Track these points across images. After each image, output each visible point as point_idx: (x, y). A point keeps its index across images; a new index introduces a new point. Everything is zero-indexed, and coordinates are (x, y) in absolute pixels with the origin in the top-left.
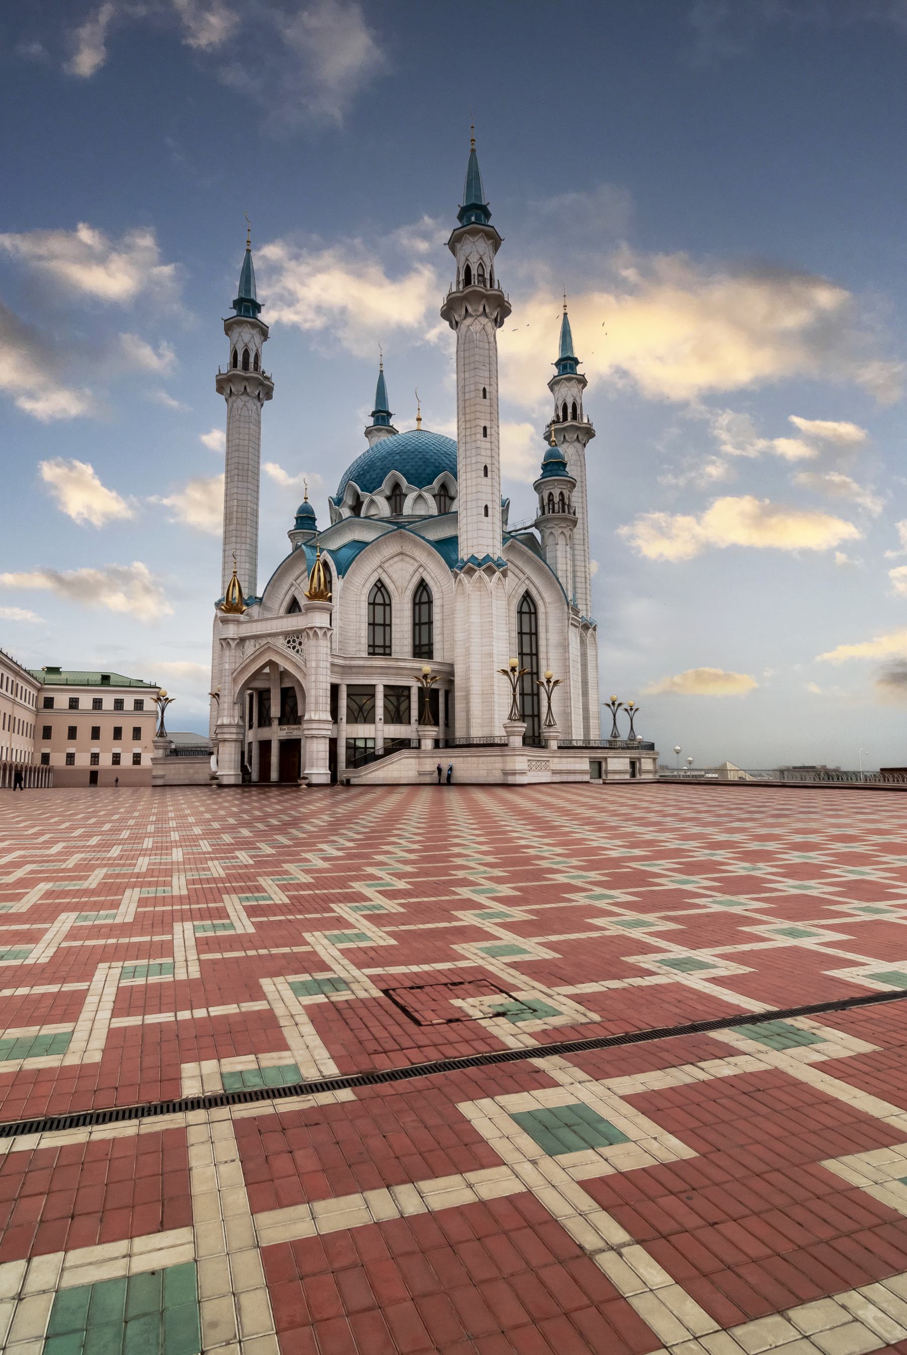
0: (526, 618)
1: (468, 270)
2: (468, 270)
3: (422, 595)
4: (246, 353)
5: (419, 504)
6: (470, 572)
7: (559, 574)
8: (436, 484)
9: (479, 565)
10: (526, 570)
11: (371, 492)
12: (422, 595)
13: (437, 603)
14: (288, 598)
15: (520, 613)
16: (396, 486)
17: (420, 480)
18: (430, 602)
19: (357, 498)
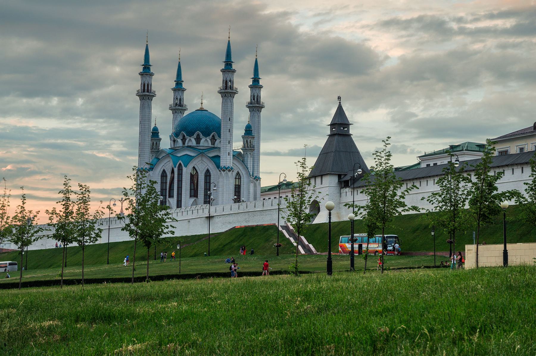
0: (237, 180)
1: (226, 81)
2: (226, 81)
3: (208, 174)
4: (148, 85)
5: (205, 142)
6: (224, 171)
7: (249, 167)
8: (211, 136)
9: (226, 169)
10: (237, 164)
11: (190, 136)
12: (208, 174)
13: (212, 177)
14: (162, 170)
15: (236, 178)
16: (198, 135)
17: (206, 134)
18: (210, 176)
19: (184, 136)
